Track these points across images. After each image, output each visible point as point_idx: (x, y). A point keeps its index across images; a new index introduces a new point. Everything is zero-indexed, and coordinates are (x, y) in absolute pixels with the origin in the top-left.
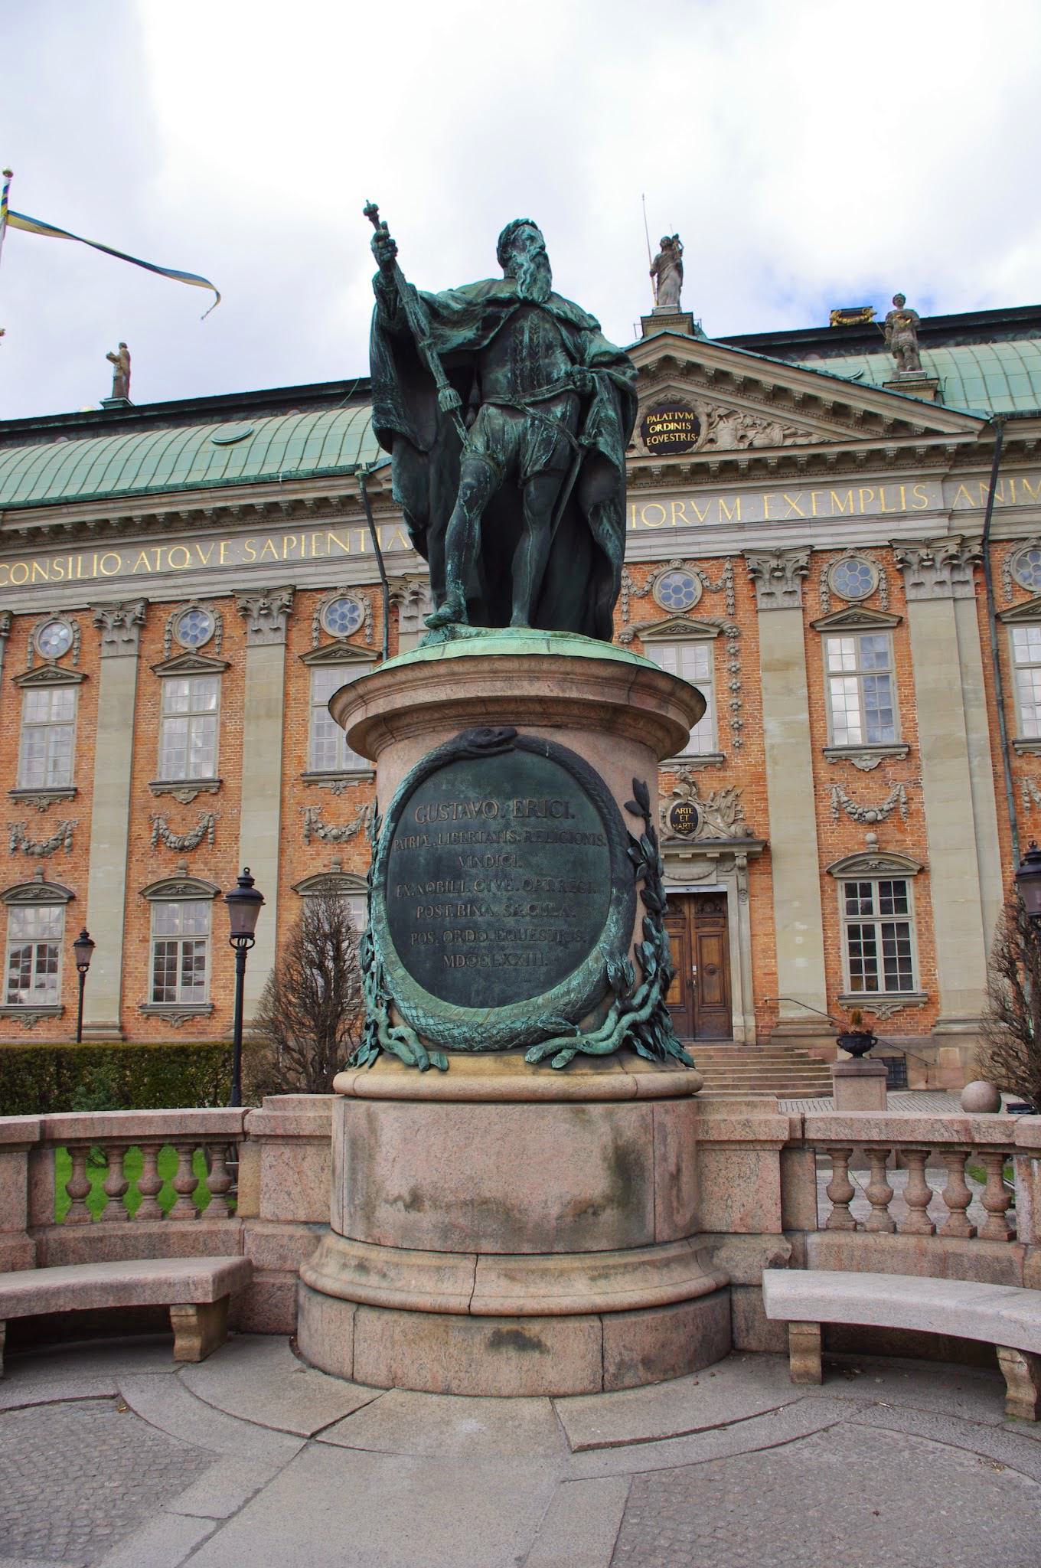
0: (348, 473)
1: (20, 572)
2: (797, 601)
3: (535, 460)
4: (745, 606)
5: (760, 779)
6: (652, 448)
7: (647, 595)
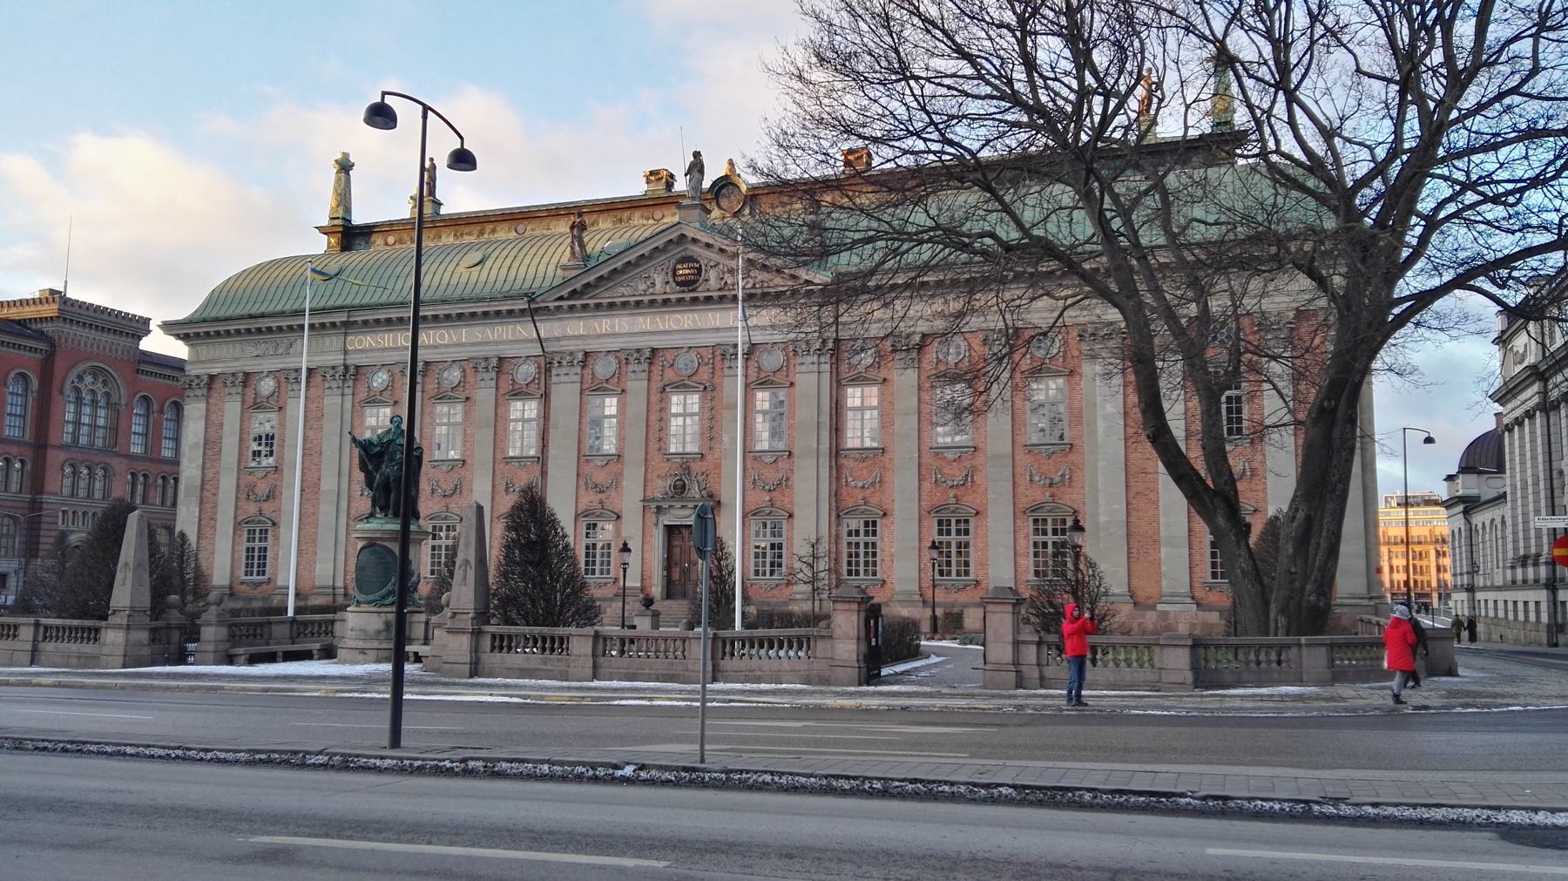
0: (519, 297)
1: (361, 342)
4: (718, 373)
5: (718, 466)
6: (678, 284)
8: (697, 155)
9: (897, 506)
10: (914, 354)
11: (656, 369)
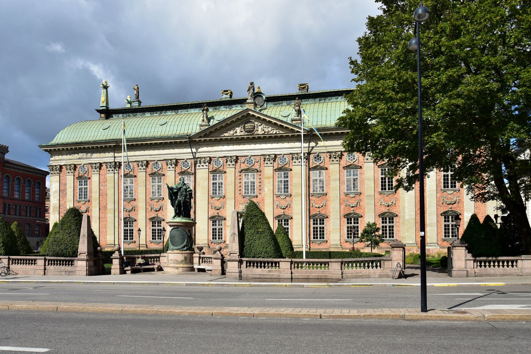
2: (272, 165)
3: (182, 202)
5: (263, 200)
6: (246, 132)
7: (244, 163)
8: (252, 84)
9: (332, 213)
10: (338, 159)
11: (238, 165)
